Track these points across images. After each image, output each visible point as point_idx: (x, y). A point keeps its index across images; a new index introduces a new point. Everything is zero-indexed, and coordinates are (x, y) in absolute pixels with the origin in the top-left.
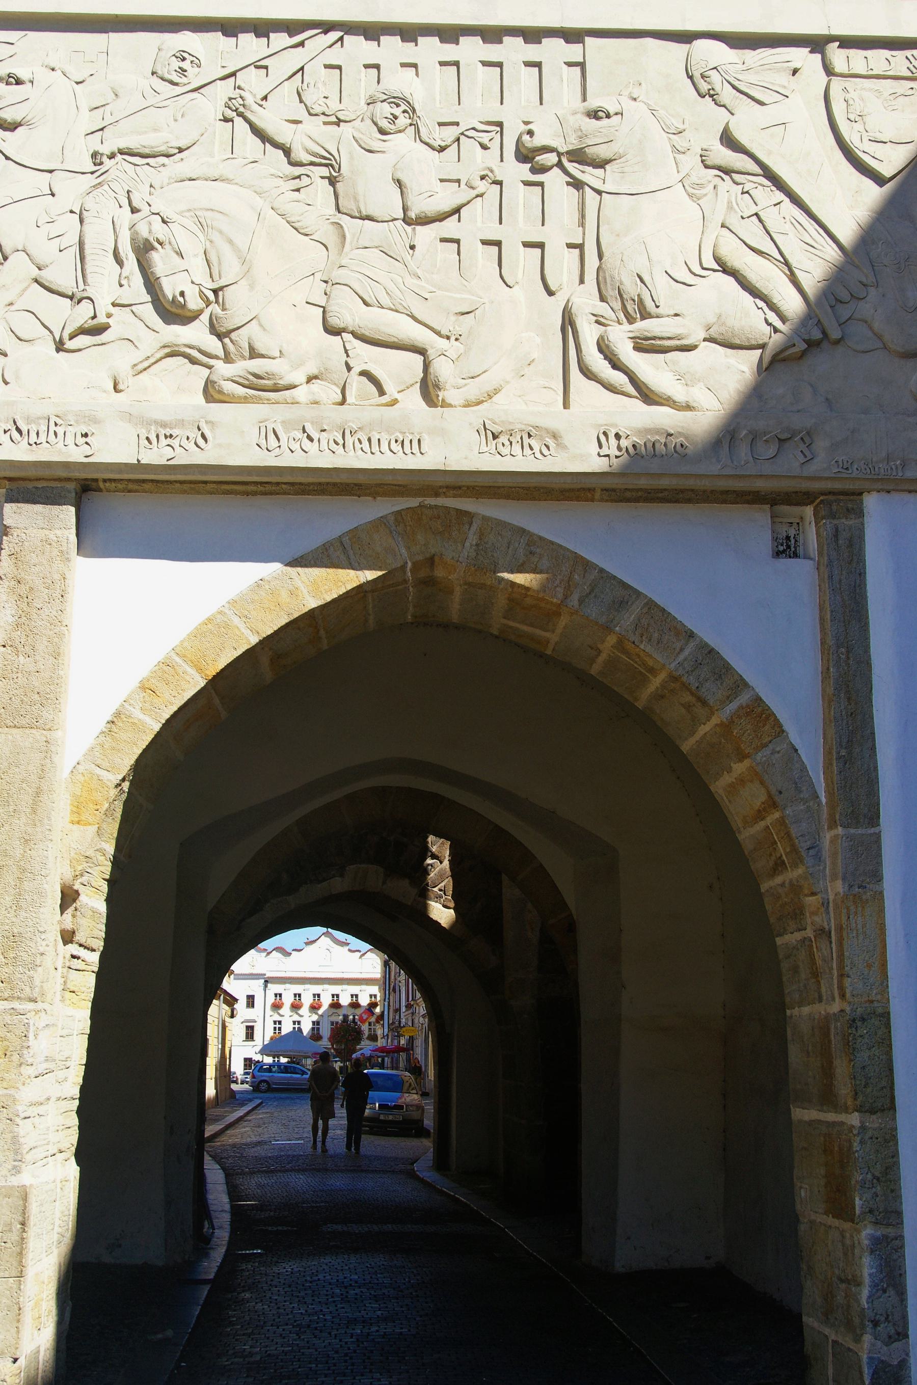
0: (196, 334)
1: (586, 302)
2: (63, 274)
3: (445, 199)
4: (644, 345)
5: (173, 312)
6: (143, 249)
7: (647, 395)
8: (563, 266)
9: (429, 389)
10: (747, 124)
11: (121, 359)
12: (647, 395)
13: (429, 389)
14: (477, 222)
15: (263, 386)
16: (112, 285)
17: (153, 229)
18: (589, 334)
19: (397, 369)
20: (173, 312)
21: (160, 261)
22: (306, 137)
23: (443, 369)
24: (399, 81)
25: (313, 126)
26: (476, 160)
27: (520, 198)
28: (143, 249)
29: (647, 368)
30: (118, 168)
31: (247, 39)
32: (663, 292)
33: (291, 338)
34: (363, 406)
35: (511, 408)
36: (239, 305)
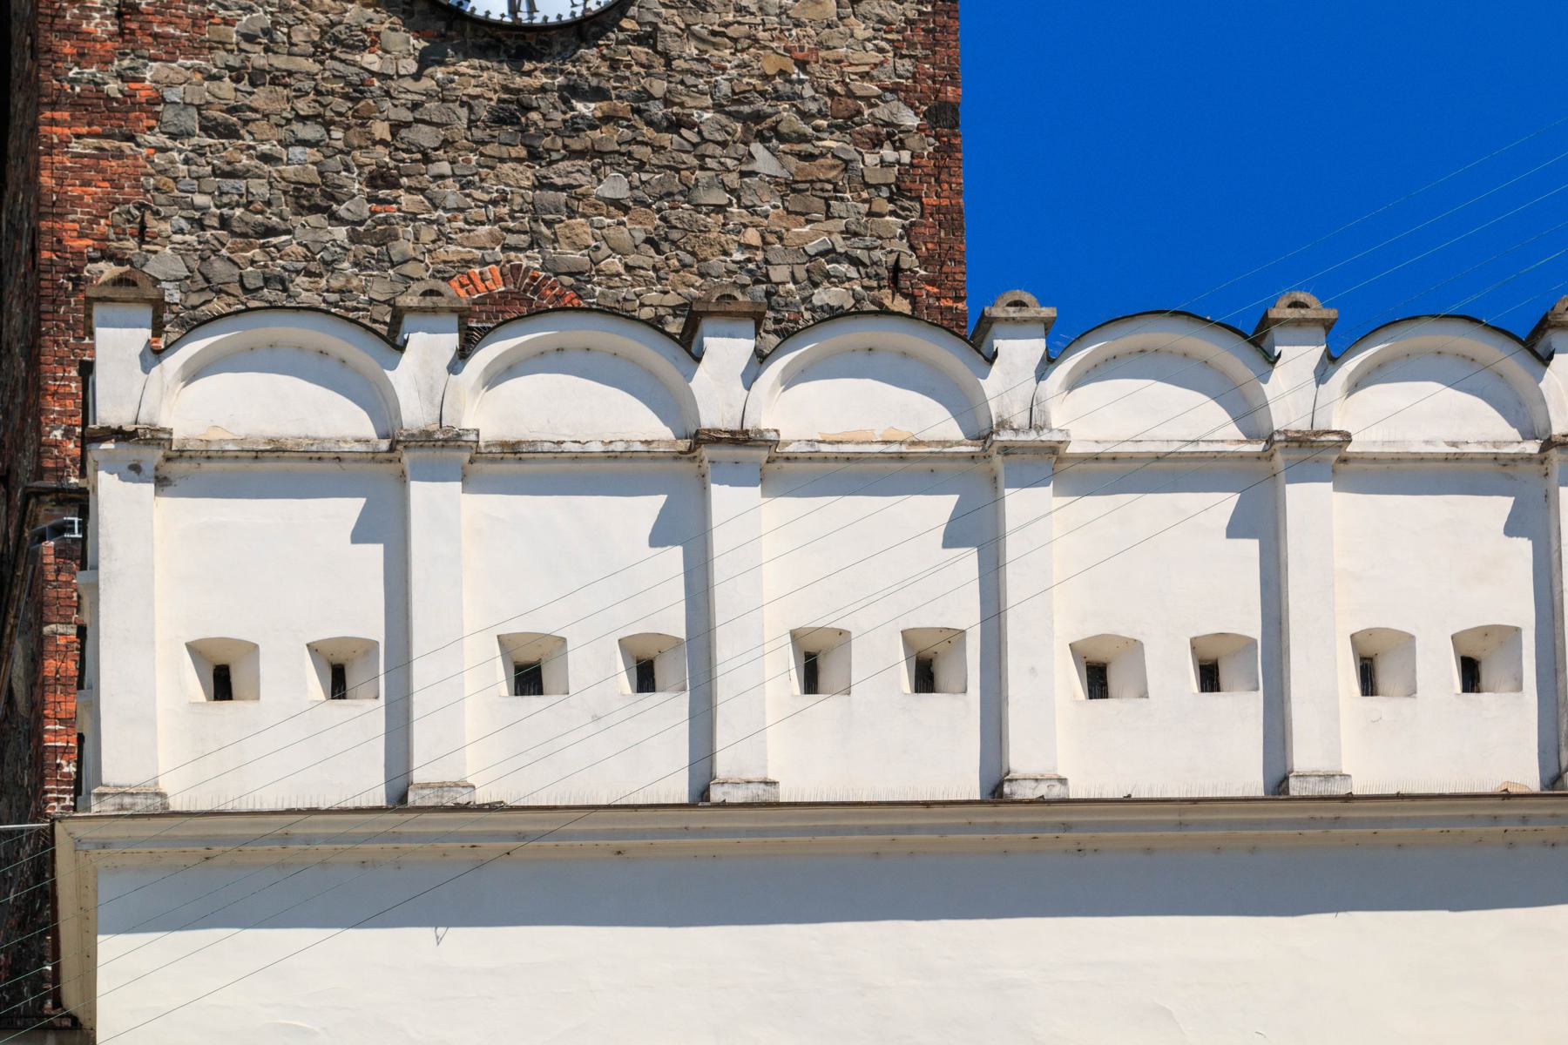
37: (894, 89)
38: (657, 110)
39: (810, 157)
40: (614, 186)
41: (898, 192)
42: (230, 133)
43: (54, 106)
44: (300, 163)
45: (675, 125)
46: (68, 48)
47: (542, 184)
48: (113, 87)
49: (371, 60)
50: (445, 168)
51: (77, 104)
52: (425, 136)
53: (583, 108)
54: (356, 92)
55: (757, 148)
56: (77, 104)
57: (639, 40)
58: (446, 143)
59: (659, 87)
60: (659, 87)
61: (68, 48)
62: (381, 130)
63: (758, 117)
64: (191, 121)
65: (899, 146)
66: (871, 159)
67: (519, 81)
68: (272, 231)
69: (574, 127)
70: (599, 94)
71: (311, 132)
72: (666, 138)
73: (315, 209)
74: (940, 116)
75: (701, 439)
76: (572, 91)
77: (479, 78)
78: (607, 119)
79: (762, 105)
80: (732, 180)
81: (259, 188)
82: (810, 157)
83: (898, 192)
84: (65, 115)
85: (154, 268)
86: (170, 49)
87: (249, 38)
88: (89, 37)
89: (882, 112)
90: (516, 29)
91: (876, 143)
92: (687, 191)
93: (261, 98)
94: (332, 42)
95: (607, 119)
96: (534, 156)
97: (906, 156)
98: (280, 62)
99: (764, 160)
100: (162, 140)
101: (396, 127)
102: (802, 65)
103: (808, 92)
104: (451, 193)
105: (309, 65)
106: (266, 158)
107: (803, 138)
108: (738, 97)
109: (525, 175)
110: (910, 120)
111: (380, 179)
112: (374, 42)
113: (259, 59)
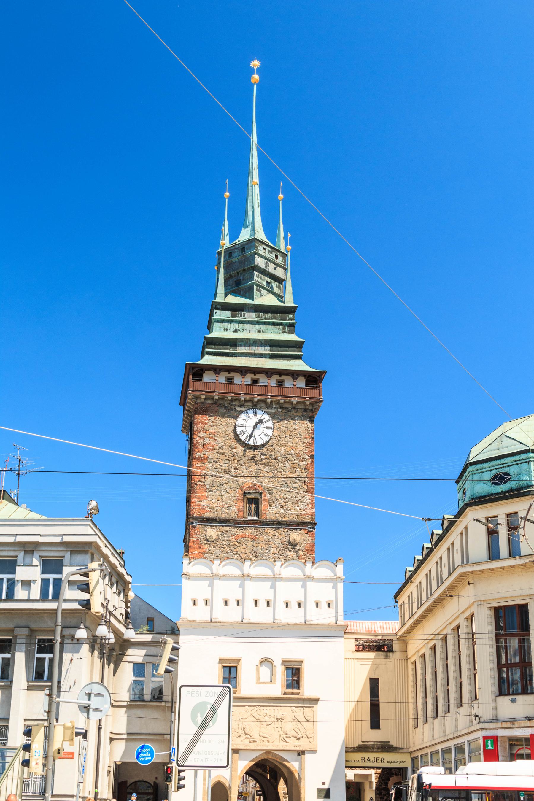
0: (248, 736)
1: (282, 733)
2: (237, 730)
3: (269, 723)
4: (287, 737)
5: (246, 734)
6: (244, 728)
7: (286, 742)
8: (280, 729)
9: (268, 742)
10: (296, 715)
11: (242, 739)
12: (286, 742)
13: (268, 742)
14: (272, 725)
15: (254, 741)
16: (241, 732)
17: (244, 727)
18: (282, 736)
19: (265, 739)
20: (246, 734)
21: (245, 730)
22: (257, 717)
23: (269, 740)
24: (266, 711)
25: (258, 716)
26: (272, 719)
27: (276, 723)
28: (244, 728)
29: (287, 740)
30: (242, 720)
31: (252, 707)
32: (288, 732)
33: (256, 737)
34: (263, 743)
35: (274, 743)
36: (252, 734)
37: (305, 453)
38: (273, 457)
39: (293, 464)
40: (267, 469)
41: (305, 469)
42: (217, 462)
43: (195, 459)
44: (225, 467)
45: (276, 459)
46: (197, 450)
47: (257, 469)
48: (202, 456)
49: (235, 450)
50: (244, 467)
51: (198, 459)
52: (242, 462)
53: (263, 457)
54: (233, 456)
55: (286, 462)
56: (198, 459)
57: (271, 446)
58: (245, 463)
59: (273, 453)
60: (273, 453)
61: (197, 450)
62: (236, 461)
63: (286, 458)
64: (212, 461)
65: (306, 462)
66: (302, 464)
67: (255, 453)
68: (221, 477)
69: (262, 460)
70: (265, 455)
71: (227, 462)
72: (274, 461)
73: (227, 473)
74: (312, 457)
75: (244, 576)
76: (262, 454)
77: (250, 453)
78: (266, 458)
79: (287, 456)
80: (283, 468)
81: (220, 470)
82: (293, 464)
83: (305, 469)
84: (196, 460)
85: (206, 483)
86: (210, 450)
87: (220, 448)
88: (199, 449)
89: (303, 457)
90: (254, 446)
91: (303, 461)
92: (277, 469)
93: (221, 457)
94: (231, 448)
95: (266, 458)
96: (256, 464)
97: (306, 463)
98: (223, 451)
99: (287, 465)
100: (208, 463)
101: (238, 461)
102: (293, 449)
103: (293, 453)
104: (245, 470)
105: (227, 452)
106: (221, 466)
107: (293, 461)
108: (284, 454)
109: (255, 467)
110: (307, 457)
111: (236, 469)
112: (236, 448)
113: (221, 451)
